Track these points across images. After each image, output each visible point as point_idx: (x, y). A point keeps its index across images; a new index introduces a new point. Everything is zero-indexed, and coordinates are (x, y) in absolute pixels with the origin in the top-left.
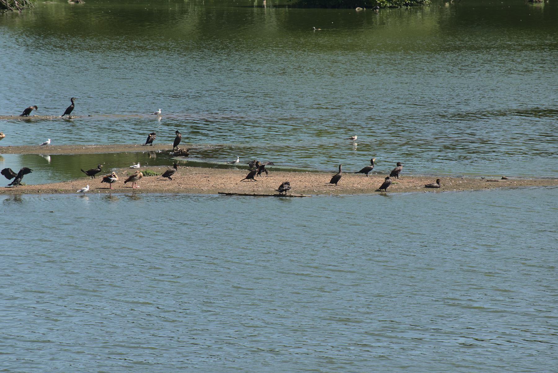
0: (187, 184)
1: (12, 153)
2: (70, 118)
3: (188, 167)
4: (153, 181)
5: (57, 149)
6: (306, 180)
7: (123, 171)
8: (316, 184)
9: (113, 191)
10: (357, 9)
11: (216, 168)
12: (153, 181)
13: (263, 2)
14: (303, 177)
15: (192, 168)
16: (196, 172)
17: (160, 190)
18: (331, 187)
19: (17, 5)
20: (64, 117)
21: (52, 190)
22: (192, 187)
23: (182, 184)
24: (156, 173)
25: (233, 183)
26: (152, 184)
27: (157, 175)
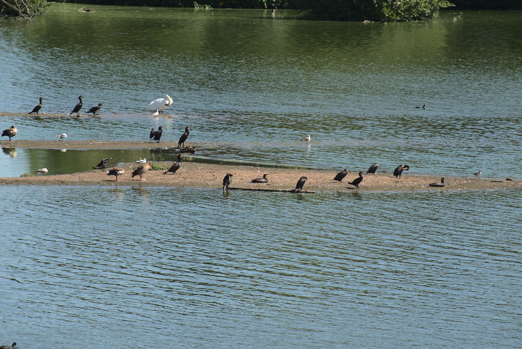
0: (192, 178)
2: (78, 116)
3: (193, 163)
4: (159, 175)
5: (64, 144)
6: (311, 177)
7: (130, 166)
8: (320, 181)
9: (119, 183)
10: (365, 22)
11: (222, 164)
12: (159, 175)
13: (271, 14)
14: (308, 174)
15: (198, 164)
16: (202, 168)
17: (165, 184)
18: (336, 184)
19: (28, 12)
20: (72, 115)
21: (59, 181)
22: (197, 181)
23: (187, 178)
24: (161, 168)
25: (238, 178)
26: (158, 178)
27: (162, 169)
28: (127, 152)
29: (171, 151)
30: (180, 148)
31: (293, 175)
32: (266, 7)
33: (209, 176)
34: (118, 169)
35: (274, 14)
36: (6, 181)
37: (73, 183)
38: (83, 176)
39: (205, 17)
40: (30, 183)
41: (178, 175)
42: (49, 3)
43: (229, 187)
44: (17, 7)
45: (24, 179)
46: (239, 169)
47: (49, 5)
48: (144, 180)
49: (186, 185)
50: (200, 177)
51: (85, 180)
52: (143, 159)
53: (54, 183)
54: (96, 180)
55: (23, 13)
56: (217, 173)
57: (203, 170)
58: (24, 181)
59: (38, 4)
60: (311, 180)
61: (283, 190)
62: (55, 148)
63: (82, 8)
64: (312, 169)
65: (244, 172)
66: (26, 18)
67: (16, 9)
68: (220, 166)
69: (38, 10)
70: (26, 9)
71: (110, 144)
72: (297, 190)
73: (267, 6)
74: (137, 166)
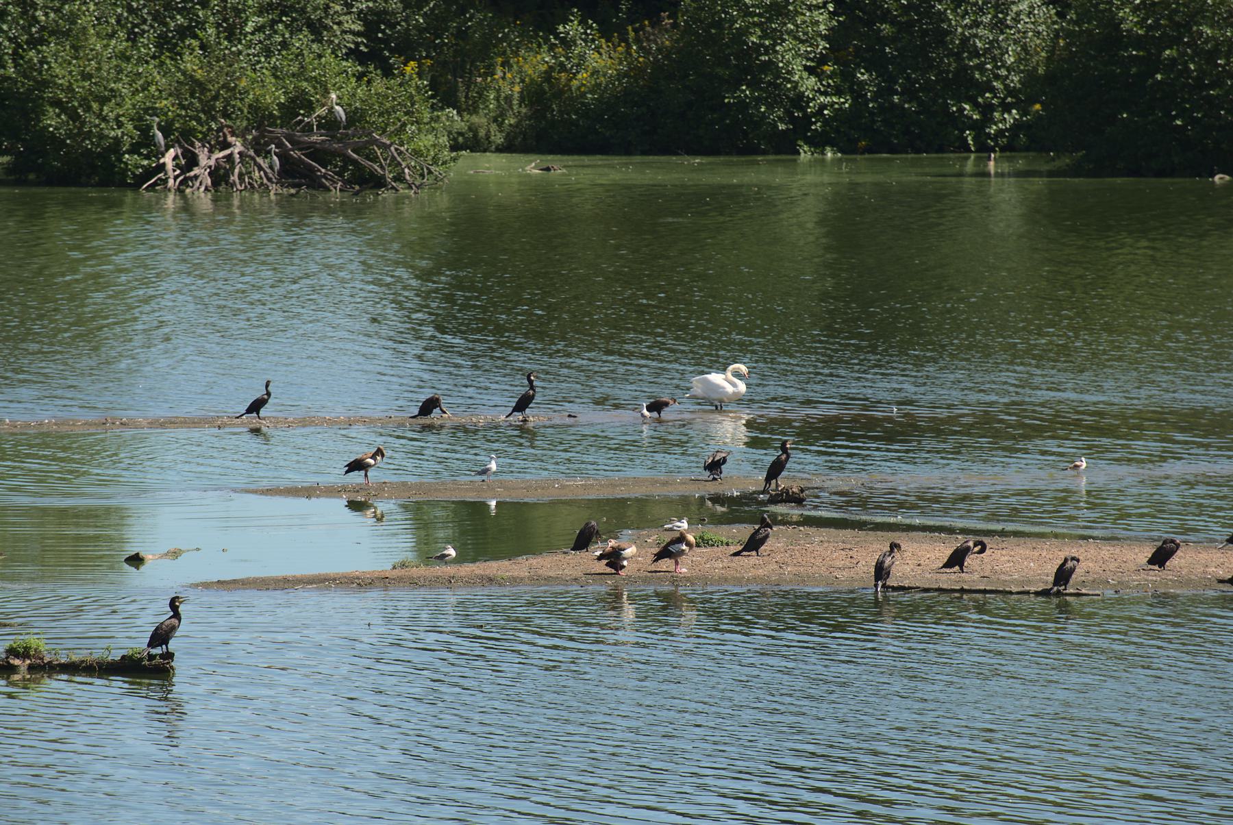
0: (799, 564)
1: (390, 498)
2: (525, 421)
3: (801, 528)
5: (493, 489)
6: (1089, 556)
7: (649, 537)
8: (1112, 566)
9: (624, 580)
10: (1217, 178)
11: (870, 529)
13: (986, 166)
14: (1082, 550)
15: (811, 530)
16: (821, 538)
17: (735, 579)
18: (1151, 572)
19: (408, 178)
20: (511, 418)
21: (482, 578)
22: (810, 570)
23: (788, 565)
24: (725, 540)
25: (910, 562)
26: (716, 565)
27: (727, 544)
28: (642, 503)
29: (747, 498)
30: (769, 493)
31: (1044, 554)
32: (973, 149)
33: (839, 558)
34: (623, 546)
35: (992, 163)
36: (358, 578)
37: (515, 581)
38: (538, 563)
39: (826, 178)
40: (414, 583)
41: (765, 558)
42: (454, 154)
43: (888, 583)
44: (382, 167)
45: (400, 574)
46: (912, 539)
47: (454, 160)
48: (684, 570)
49: (785, 580)
50: (818, 562)
51: (543, 572)
52: (679, 521)
53: (469, 582)
54: (569, 572)
55: (395, 179)
56: (860, 550)
57: (826, 545)
58: (400, 579)
59: (429, 158)
60: (1091, 565)
61: (1020, 589)
62: (471, 497)
63: (533, 164)
64: (1094, 538)
65: (925, 546)
66: (401, 191)
67: (379, 170)
68: (867, 534)
69: (430, 172)
70: (403, 169)
71: (601, 485)
72: (1055, 588)
73: (974, 145)
74: (667, 538)
